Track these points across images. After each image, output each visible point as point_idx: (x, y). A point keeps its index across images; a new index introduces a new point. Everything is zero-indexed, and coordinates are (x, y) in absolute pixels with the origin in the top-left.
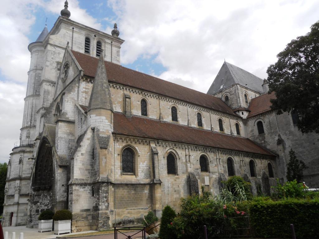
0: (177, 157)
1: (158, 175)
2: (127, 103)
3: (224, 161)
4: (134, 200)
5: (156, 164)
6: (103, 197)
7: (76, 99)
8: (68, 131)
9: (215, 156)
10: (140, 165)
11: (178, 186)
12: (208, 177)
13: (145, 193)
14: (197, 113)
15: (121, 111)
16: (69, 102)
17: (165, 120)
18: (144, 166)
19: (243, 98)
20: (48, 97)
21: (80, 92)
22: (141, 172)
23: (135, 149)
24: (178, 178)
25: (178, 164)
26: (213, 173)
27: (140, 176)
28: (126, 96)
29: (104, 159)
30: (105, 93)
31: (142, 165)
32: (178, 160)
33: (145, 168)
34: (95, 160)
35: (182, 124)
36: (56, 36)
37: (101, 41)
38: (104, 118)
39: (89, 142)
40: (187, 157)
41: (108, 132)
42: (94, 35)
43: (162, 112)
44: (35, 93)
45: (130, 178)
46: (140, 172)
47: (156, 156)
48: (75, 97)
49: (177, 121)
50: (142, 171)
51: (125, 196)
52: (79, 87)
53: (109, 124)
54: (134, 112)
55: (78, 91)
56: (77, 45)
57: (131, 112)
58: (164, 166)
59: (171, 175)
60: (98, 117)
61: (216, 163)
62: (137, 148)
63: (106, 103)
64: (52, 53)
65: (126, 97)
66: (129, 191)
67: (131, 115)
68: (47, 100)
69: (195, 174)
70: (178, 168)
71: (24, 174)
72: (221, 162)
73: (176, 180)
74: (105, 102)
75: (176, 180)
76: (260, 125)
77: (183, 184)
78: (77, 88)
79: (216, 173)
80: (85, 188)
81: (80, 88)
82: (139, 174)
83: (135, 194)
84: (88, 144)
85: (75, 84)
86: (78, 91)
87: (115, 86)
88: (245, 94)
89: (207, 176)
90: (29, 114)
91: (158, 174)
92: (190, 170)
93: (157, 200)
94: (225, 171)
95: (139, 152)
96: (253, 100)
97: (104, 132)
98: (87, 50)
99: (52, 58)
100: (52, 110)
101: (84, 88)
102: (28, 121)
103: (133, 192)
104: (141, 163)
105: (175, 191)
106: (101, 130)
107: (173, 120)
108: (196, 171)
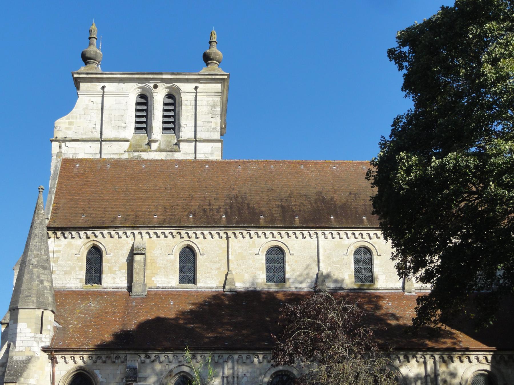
14: (353, 249)
23: (93, 373)
41: (30, 351)
53: (33, 335)
54: (158, 281)
57: (144, 285)
62: (97, 372)
63: (30, 296)
74: (27, 296)
97: (22, 351)
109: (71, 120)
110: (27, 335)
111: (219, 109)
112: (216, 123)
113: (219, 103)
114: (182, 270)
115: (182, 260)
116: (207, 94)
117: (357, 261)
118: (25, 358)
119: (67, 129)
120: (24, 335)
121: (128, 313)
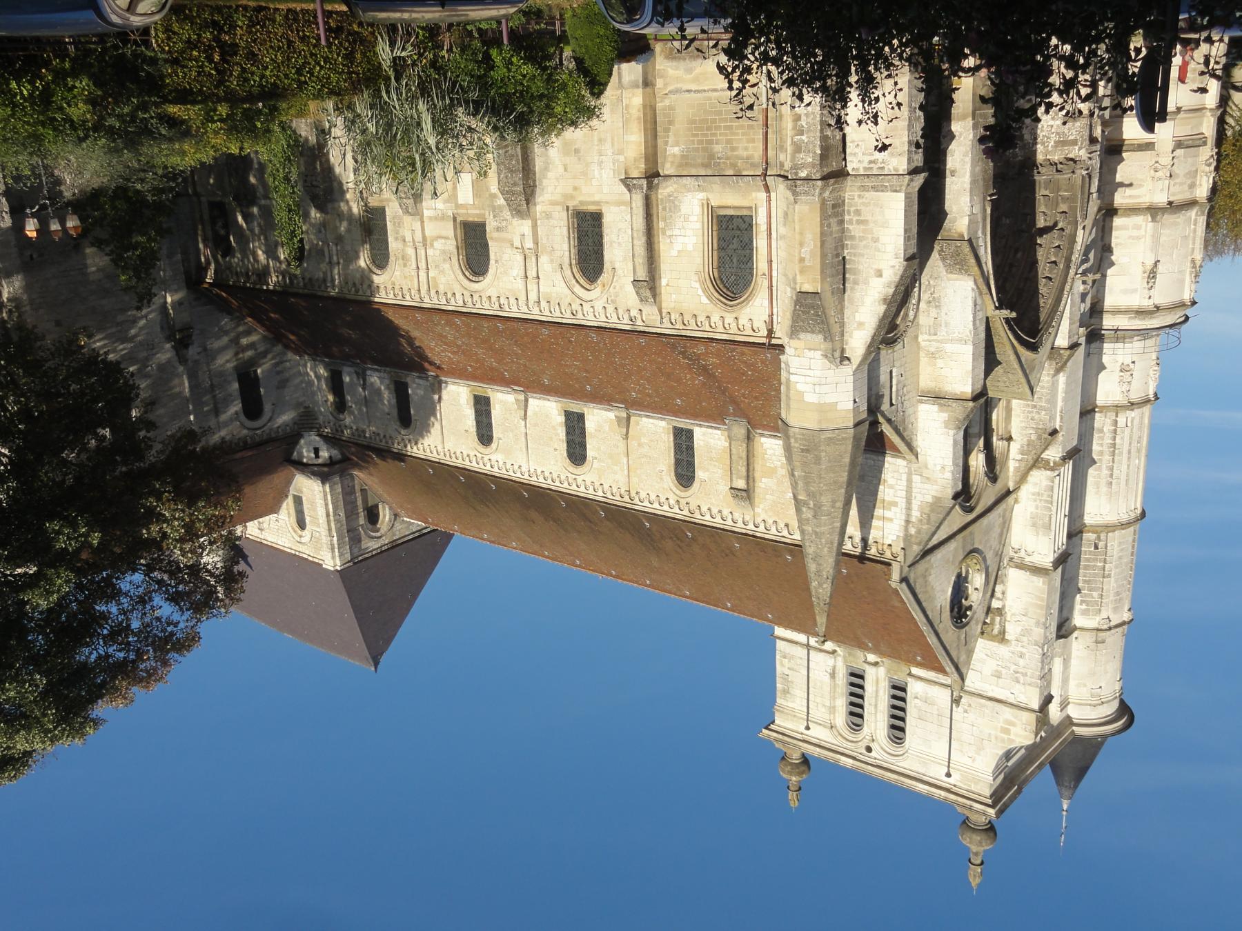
0: (568, 272)
1: (634, 205)
2: (744, 470)
3: (401, 261)
4: (714, 121)
5: (641, 242)
6: (809, 130)
7: (916, 478)
8: (940, 363)
9: (434, 278)
10: (694, 240)
11: (566, 170)
12: (460, 201)
13: (677, 144)
14: (494, 445)
15: (763, 440)
16: (939, 468)
17: (611, 415)
18: (680, 239)
19: (312, 513)
20: (1037, 508)
21: (902, 503)
22: (691, 219)
24: (566, 196)
25: (566, 247)
26: (443, 218)
27: (696, 202)
28: (744, 494)
29: (808, 257)
30: (807, 484)
31: (687, 242)
32: (567, 261)
33: (676, 232)
34: (837, 255)
35: (547, 403)
36: (1012, 741)
37: (846, 732)
38: (810, 398)
39: (858, 317)
40: (532, 273)
42: (873, 754)
43: (622, 444)
44: (1103, 536)
45: (730, 199)
46: (695, 218)
47: (642, 274)
48: (919, 485)
49: (568, 415)
50: (686, 218)
51: (743, 134)
52: (908, 522)
53: (793, 378)
55: (909, 508)
56: (936, 712)
58: (614, 238)
59: (592, 208)
60: (830, 399)
61: (430, 252)
62: (705, 300)
63: (803, 451)
64: (1025, 675)
65: (745, 494)
66: (730, 153)
67: (729, 430)
68: (1038, 494)
69: (507, 214)
70: (565, 233)
71: (1138, 227)
72: (414, 257)
73: (575, 189)
74: (807, 451)
75: (575, 189)
76: (253, 408)
77: (550, 175)
78: (913, 519)
79: (430, 218)
80: (871, 162)
81: (904, 517)
82: (697, 210)
83: (710, 142)
84: (862, 310)
85: (919, 532)
86: (909, 508)
87: (785, 533)
88: (304, 533)
89: (462, 206)
90: (1125, 455)
91: (635, 211)
92: (525, 226)
93: (639, 118)
94: (398, 224)
95: (697, 285)
96: (274, 509)
97: (810, 349)
98: (899, 692)
99: (1022, 656)
100: (1020, 457)
101: (891, 520)
102: (1127, 431)
103: (718, 148)
104: (690, 248)
105: (577, 151)
106: (818, 354)
107: (581, 417)
108: (504, 224)
109: (1006, 737)
110: (801, 379)
111: (779, 686)
112: (783, 665)
113: (778, 694)
114: (690, 449)
115: (690, 465)
116: (793, 714)
117: (490, 426)
118: (802, 335)
119: (1013, 724)
120: (808, 380)
121: (724, 393)
